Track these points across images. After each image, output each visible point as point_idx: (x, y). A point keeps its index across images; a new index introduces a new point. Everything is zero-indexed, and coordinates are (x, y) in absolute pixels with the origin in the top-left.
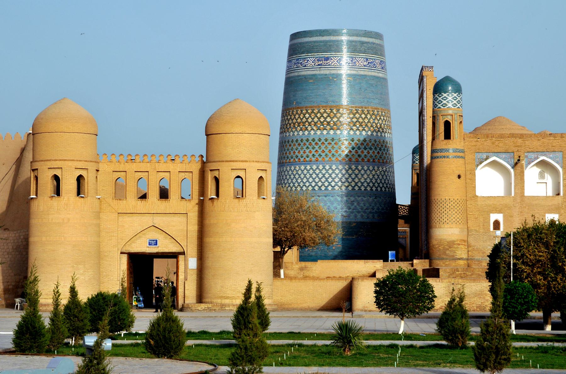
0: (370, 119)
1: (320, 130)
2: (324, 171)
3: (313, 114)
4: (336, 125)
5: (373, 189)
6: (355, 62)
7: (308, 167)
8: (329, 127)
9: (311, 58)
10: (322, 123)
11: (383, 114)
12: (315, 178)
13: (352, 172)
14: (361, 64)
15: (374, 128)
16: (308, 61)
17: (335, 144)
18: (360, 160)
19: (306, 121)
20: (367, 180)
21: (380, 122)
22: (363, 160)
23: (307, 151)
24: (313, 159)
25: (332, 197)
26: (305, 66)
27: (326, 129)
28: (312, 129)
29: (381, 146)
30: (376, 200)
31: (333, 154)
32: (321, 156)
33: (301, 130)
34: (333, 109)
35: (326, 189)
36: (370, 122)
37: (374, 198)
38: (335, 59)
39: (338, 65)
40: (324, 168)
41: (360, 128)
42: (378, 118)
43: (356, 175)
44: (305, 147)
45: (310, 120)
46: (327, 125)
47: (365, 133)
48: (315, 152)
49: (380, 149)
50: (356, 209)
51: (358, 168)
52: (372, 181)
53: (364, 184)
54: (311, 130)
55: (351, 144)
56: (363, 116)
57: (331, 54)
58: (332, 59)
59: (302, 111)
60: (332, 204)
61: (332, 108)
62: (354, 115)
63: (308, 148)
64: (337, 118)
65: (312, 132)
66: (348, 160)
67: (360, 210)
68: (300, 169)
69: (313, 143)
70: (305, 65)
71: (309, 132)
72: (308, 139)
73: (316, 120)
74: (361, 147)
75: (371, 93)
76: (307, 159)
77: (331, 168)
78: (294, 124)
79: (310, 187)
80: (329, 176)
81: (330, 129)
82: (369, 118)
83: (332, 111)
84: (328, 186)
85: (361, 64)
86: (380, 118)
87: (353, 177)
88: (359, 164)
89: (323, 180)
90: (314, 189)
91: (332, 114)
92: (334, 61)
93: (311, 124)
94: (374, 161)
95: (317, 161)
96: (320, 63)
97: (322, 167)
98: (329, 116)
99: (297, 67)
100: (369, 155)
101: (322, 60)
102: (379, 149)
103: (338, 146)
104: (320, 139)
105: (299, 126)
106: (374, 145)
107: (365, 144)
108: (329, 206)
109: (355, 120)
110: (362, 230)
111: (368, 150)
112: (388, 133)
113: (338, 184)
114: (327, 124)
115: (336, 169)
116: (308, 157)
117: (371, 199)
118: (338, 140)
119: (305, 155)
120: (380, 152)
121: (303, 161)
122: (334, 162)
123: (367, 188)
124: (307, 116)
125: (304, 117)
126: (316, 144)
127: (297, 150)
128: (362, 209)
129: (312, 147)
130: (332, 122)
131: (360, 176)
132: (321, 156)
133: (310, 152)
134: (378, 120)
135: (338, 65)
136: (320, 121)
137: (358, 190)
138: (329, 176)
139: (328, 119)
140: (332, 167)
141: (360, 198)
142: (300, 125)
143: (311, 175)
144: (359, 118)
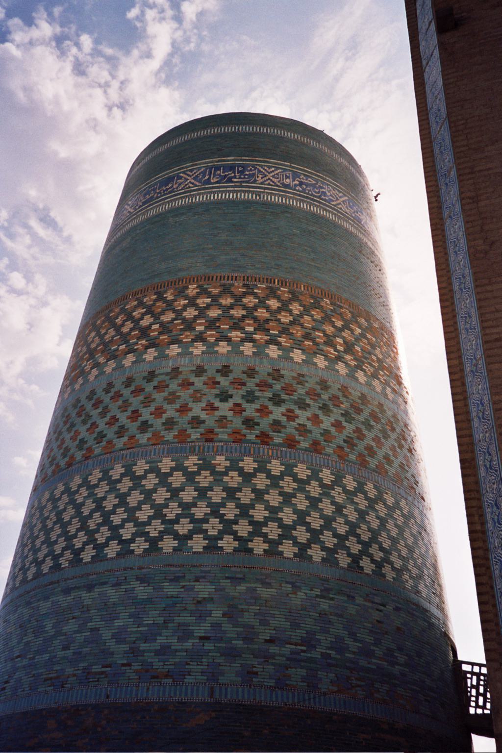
0: (301, 316)
13: (211, 479)
18: (252, 437)
25: (117, 585)
30: (324, 605)
38: (191, 174)
50: (221, 640)
53: (265, 530)
55: (218, 383)
58: (181, 178)
66: (198, 436)
67: (239, 643)
85: (275, 180)
87: (216, 499)
94: (316, 447)
108: (98, 629)
118: (167, 374)
128: (247, 639)
135: (196, 186)
137: (235, 550)
141: (242, 588)
144: (255, 308)
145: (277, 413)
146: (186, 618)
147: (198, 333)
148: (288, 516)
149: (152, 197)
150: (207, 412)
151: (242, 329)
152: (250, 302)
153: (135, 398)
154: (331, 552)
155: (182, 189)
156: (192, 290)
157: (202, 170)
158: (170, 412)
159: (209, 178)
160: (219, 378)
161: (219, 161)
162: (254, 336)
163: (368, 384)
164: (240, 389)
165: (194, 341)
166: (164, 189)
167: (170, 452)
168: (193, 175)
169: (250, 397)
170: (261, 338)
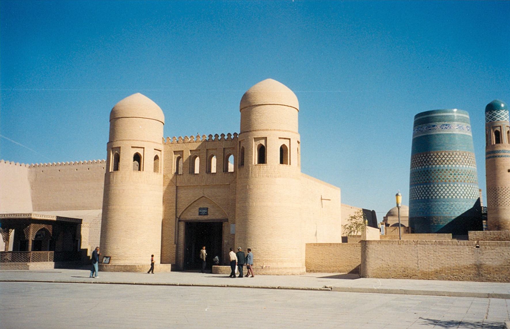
3: (427, 157)
4: (440, 162)
6: (451, 127)
7: (425, 186)
11: (470, 155)
15: (464, 163)
16: (423, 128)
19: (423, 161)
21: (468, 159)
22: (457, 181)
24: (428, 181)
26: (422, 131)
28: (427, 165)
31: (439, 178)
33: (420, 166)
42: (467, 157)
43: (454, 190)
44: (423, 175)
45: (425, 160)
49: (468, 175)
56: (457, 156)
58: (437, 126)
59: (420, 155)
60: (440, 206)
62: (451, 156)
63: (424, 175)
65: (427, 167)
68: (420, 187)
71: (425, 166)
76: (425, 182)
78: (417, 163)
84: (437, 196)
86: (468, 158)
88: (455, 183)
98: (436, 157)
99: (418, 132)
100: (461, 178)
111: (461, 175)
112: (473, 166)
122: (439, 183)
125: (422, 158)
130: (438, 160)
139: (436, 159)
141: (456, 203)
143: (426, 191)
145: (459, 176)
146: (450, 207)
148: (461, 193)
151: (452, 162)
167: (445, 183)
169: (455, 174)
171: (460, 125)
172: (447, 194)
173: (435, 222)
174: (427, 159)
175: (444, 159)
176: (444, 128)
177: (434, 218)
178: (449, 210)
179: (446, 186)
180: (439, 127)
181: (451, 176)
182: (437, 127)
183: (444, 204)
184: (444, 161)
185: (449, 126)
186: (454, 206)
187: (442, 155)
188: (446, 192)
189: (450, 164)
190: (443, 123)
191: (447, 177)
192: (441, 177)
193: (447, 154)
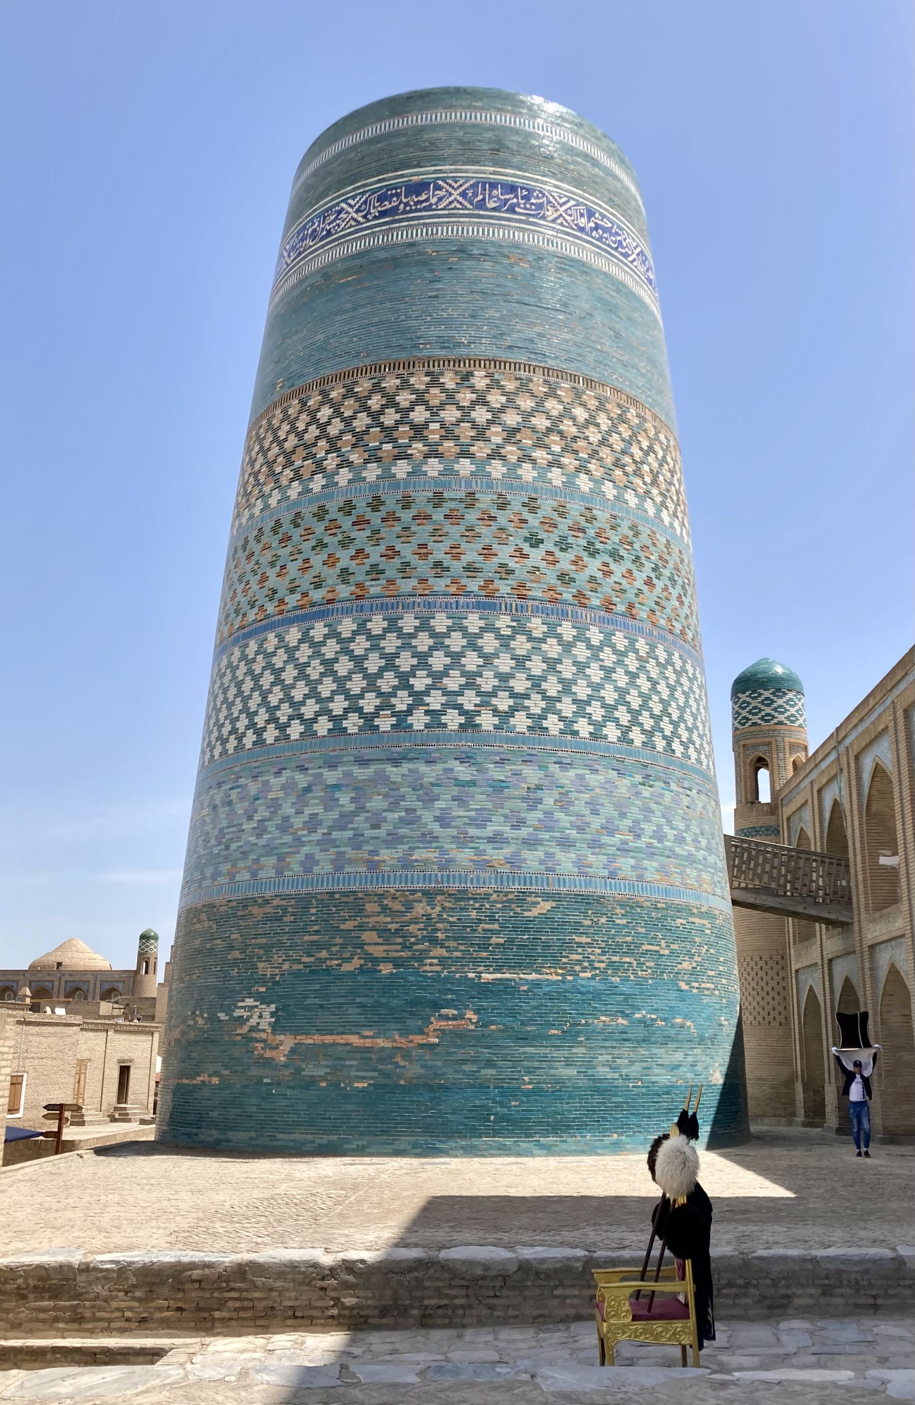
0: (609, 433)
1: (379, 460)
2: (391, 643)
5: (631, 735)
6: (540, 206)
8: (419, 445)
9: (353, 198)
10: (389, 433)
12: (348, 678)
14: (567, 217)
15: (626, 474)
17: (446, 517)
18: (568, 597)
19: (318, 438)
20: (603, 693)
23: (317, 560)
24: (344, 591)
25: (429, 762)
26: (329, 233)
27: (408, 457)
28: (345, 463)
29: (661, 558)
30: (646, 792)
31: (438, 564)
32: (382, 572)
33: (297, 476)
34: (442, 374)
35: (402, 719)
36: (610, 446)
37: (639, 778)
38: (456, 186)
39: (466, 208)
40: (393, 626)
41: (565, 460)
43: (552, 664)
46: (411, 439)
47: (591, 485)
48: (352, 558)
51: (559, 630)
52: (628, 698)
53: (589, 710)
54: (340, 466)
57: (435, 172)
58: (440, 188)
59: (303, 403)
60: (429, 800)
61: (436, 369)
63: (321, 545)
64: (460, 408)
65: (344, 476)
67: (573, 833)
69: (346, 523)
70: (329, 232)
72: (322, 508)
73: (362, 421)
74: (571, 540)
75: (609, 337)
76: (317, 595)
77: (424, 625)
79: (323, 719)
80: (415, 661)
81: (427, 456)
82: (604, 427)
83: (434, 382)
84: (409, 711)
85: (567, 217)
86: (651, 449)
89: (388, 682)
90: (338, 730)
91: (435, 391)
92: (451, 194)
93: (339, 444)
95: (359, 597)
96: (387, 205)
97: (385, 624)
98: (421, 399)
99: (300, 253)
101: (398, 195)
102: (654, 570)
103: (462, 528)
104: (377, 498)
105: (289, 463)
106: (631, 544)
107: (591, 532)
109: (540, 422)
110: (584, 939)
113: (460, 700)
114: (412, 433)
115: (450, 629)
116: (318, 586)
117: (626, 782)
118: (461, 501)
119: (305, 581)
120: (655, 581)
121: (295, 608)
123: (605, 731)
124: (325, 413)
126: (360, 522)
127: (272, 564)
128: (580, 829)
129: (340, 537)
130: (434, 426)
131: (567, 670)
132: (382, 572)
133: (331, 561)
134: (641, 449)
135: (466, 208)
136: (381, 425)
138: (415, 661)
139: (419, 415)
140: (432, 622)
141: (571, 773)
142: (293, 457)
145: (593, 566)
147: (494, 447)
149: (397, 207)
150: (516, 559)
152: (553, 408)
153: (420, 527)
154: (649, 734)
155: (444, 209)
156: (480, 380)
157: (472, 182)
158: (471, 555)
159: (484, 199)
160: (526, 515)
161: (495, 173)
162: (562, 459)
163: (641, 508)
164: (552, 532)
165: (491, 457)
166: (416, 200)
167: (479, 606)
168: (458, 188)
169: (564, 545)
170: (570, 463)
171: (603, 216)
172: (494, 694)
173: (378, 951)
174: (348, 421)
175: (481, 415)
176: (491, 205)
177: (371, 907)
178: (507, 830)
179: (489, 628)
180: (455, 195)
181: (536, 556)
182: (440, 193)
183: (473, 783)
184: (481, 434)
185: (526, 198)
186: (549, 801)
187: (474, 390)
188: (487, 682)
189: (526, 458)
190: (488, 171)
191: (504, 554)
192: (455, 552)
193: (510, 386)
